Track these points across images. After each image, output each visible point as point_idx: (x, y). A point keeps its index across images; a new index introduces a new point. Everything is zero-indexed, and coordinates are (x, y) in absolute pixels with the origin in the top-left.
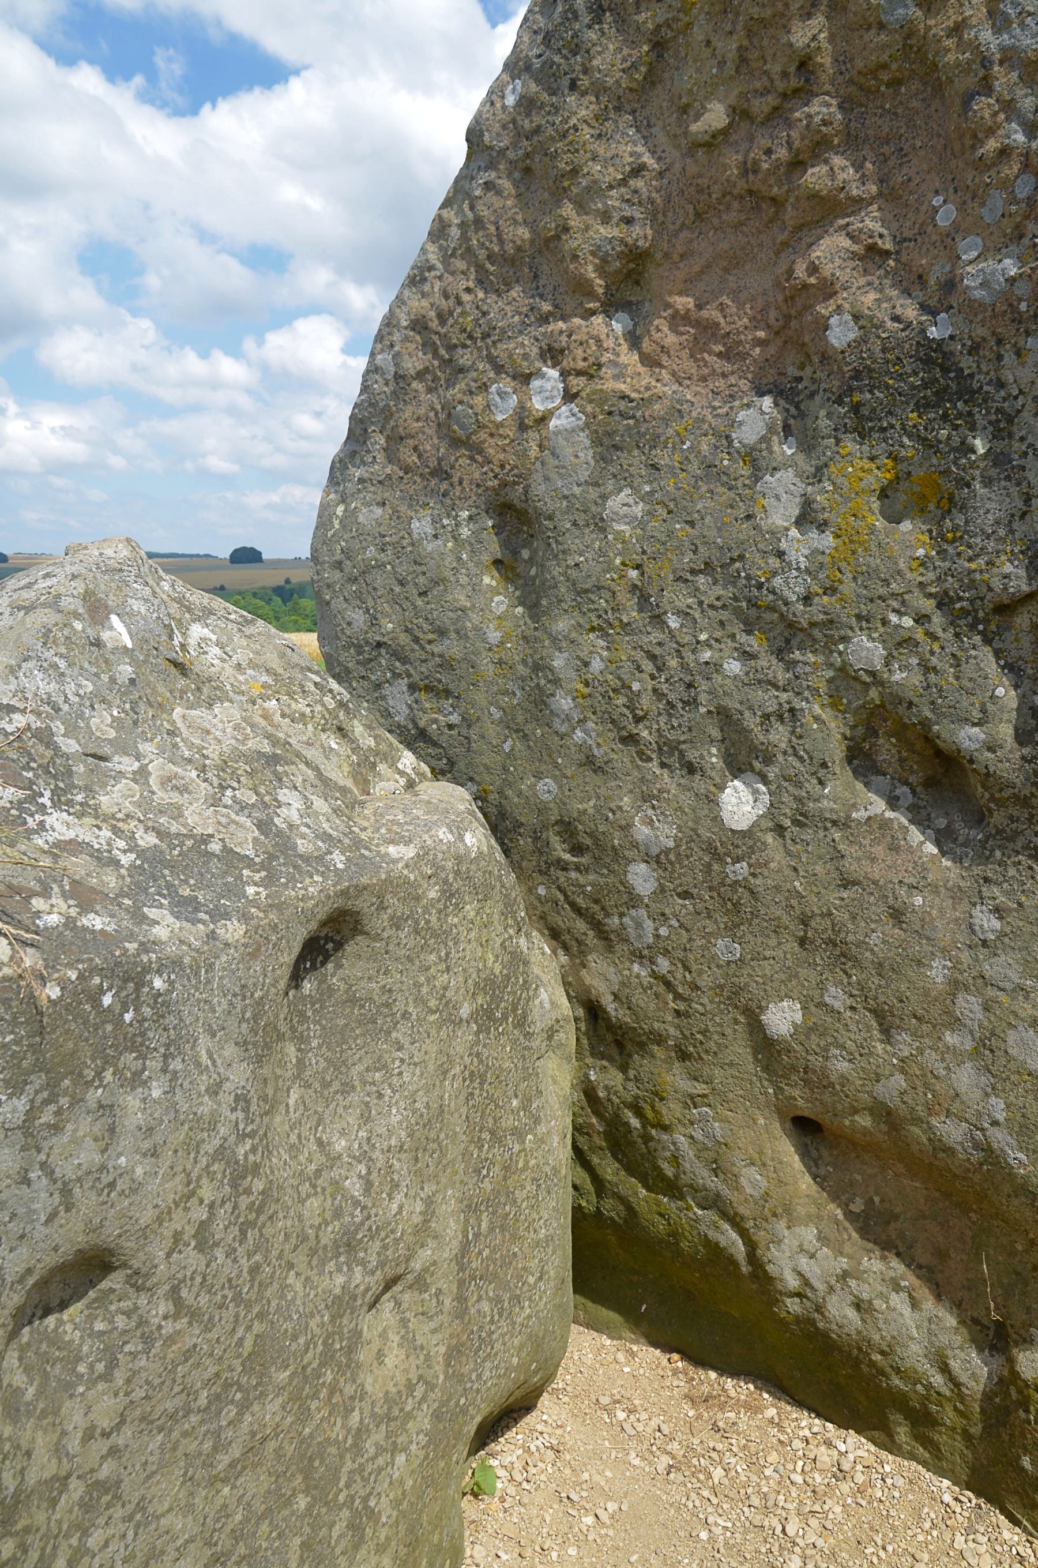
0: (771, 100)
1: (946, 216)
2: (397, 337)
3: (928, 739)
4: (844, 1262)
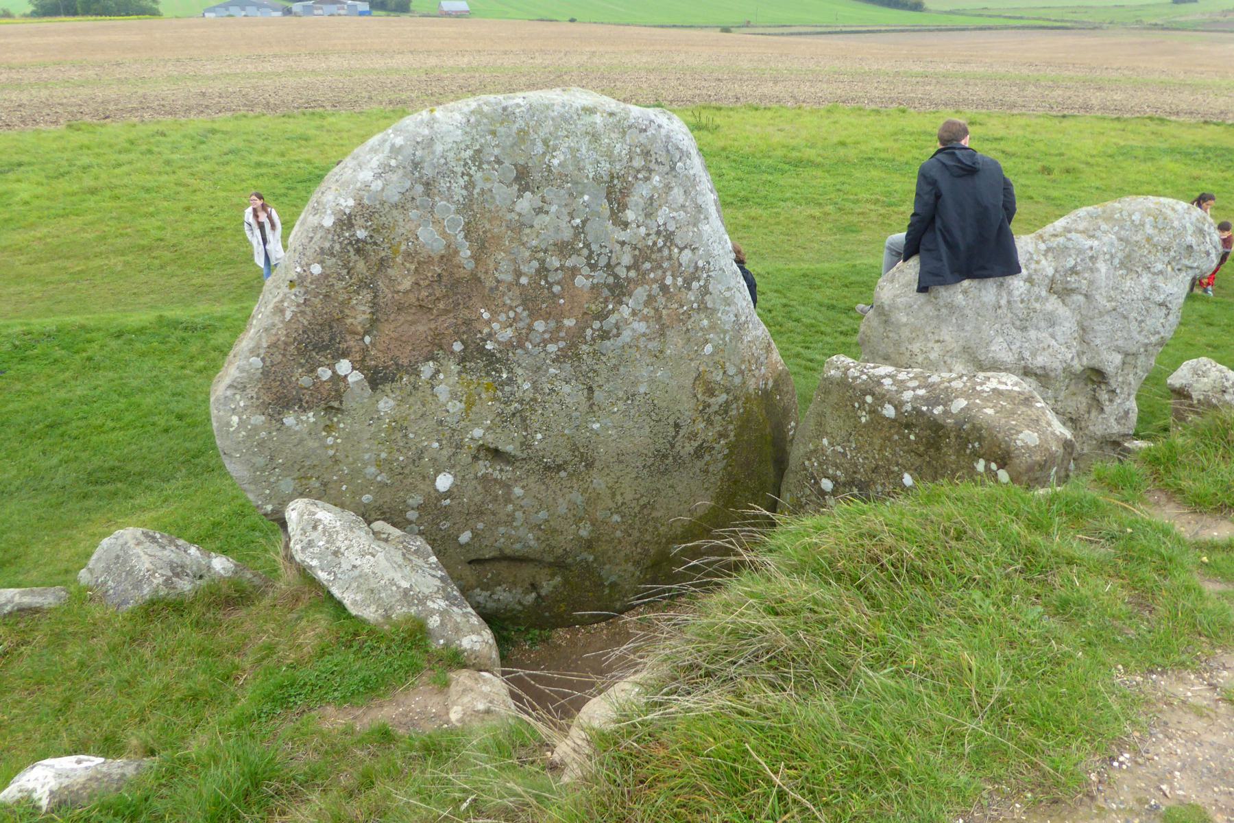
0: (427, 282)
1: (486, 315)
2: (262, 351)
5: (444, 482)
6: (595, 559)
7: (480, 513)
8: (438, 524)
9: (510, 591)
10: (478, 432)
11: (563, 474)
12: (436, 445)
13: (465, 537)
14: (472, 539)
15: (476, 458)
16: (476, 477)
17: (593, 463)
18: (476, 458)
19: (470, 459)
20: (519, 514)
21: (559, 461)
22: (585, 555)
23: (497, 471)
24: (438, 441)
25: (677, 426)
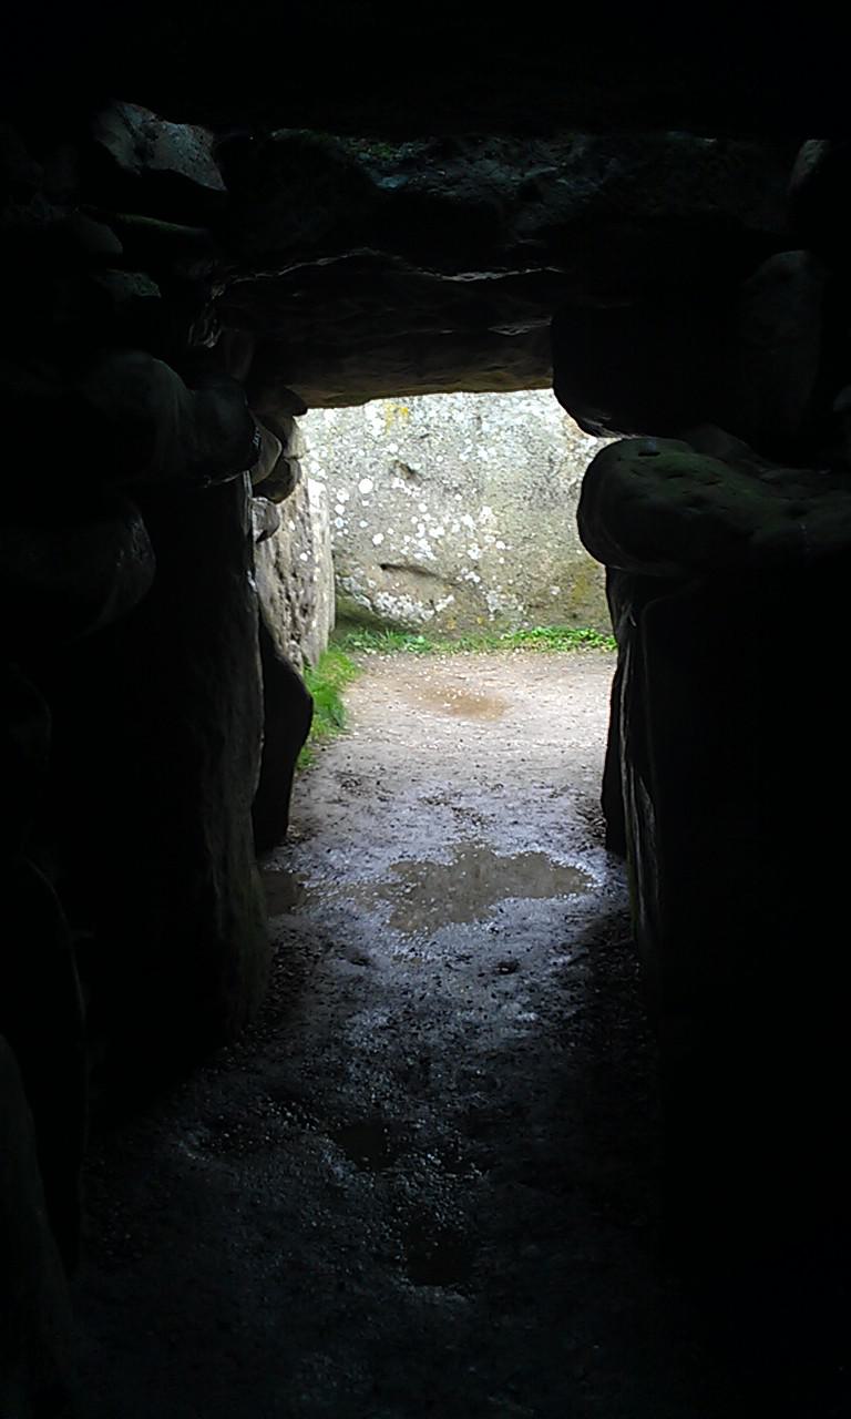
3: (408, 467)
4: (395, 599)
5: (366, 486)
6: (481, 582)
8: (358, 522)
9: (413, 604)
10: (393, 448)
11: (458, 497)
12: (362, 453)
13: (378, 539)
14: (383, 542)
16: (391, 489)
17: (483, 489)
19: (386, 471)
20: (421, 527)
22: (472, 575)
23: (409, 489)
24: (365, 450)
25: (550, 460)
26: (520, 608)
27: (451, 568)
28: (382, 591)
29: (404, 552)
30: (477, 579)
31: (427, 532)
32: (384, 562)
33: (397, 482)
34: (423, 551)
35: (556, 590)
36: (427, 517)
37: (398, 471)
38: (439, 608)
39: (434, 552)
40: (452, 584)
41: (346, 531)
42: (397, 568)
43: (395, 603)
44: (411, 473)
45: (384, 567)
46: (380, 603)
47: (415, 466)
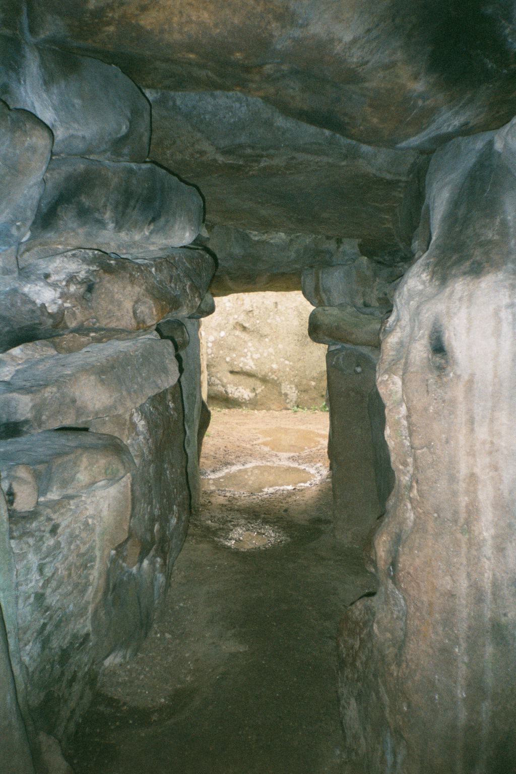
3: (242, 325)
7: (234, 349)
11: (267, 340)
15: (235, 328)
18: (235, 328)
20: (249, 354)
21: (266, 333)
23: (244, 336)
26: (297, 392)
27: (263, 373)
28: (230, 384)
29: (241, 365)
30: (276, 378)
31: (251, 356)
32: (231, 370)
33: (238, 333)
34: (249, 365)
35: (313, 383)
36: (252, 349)
37: (238, 327)
38: (257, 392)
39: (255, 365)
40: (264, 380)
41: (213, 355)
42: (237, 373)
43: (237, 389)
44: (244, 328)
45: (232, 372)
46: (229, 391)
47: (247, 325)
